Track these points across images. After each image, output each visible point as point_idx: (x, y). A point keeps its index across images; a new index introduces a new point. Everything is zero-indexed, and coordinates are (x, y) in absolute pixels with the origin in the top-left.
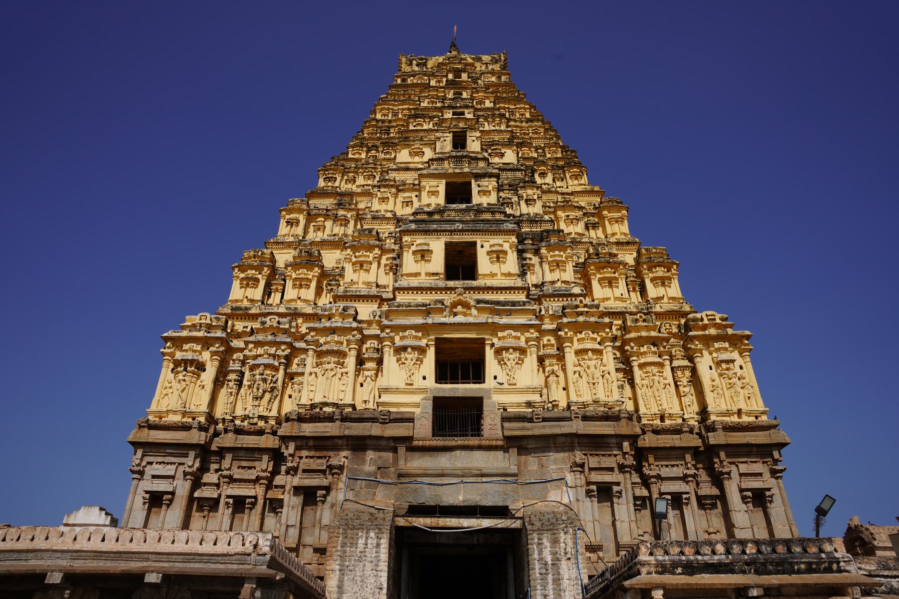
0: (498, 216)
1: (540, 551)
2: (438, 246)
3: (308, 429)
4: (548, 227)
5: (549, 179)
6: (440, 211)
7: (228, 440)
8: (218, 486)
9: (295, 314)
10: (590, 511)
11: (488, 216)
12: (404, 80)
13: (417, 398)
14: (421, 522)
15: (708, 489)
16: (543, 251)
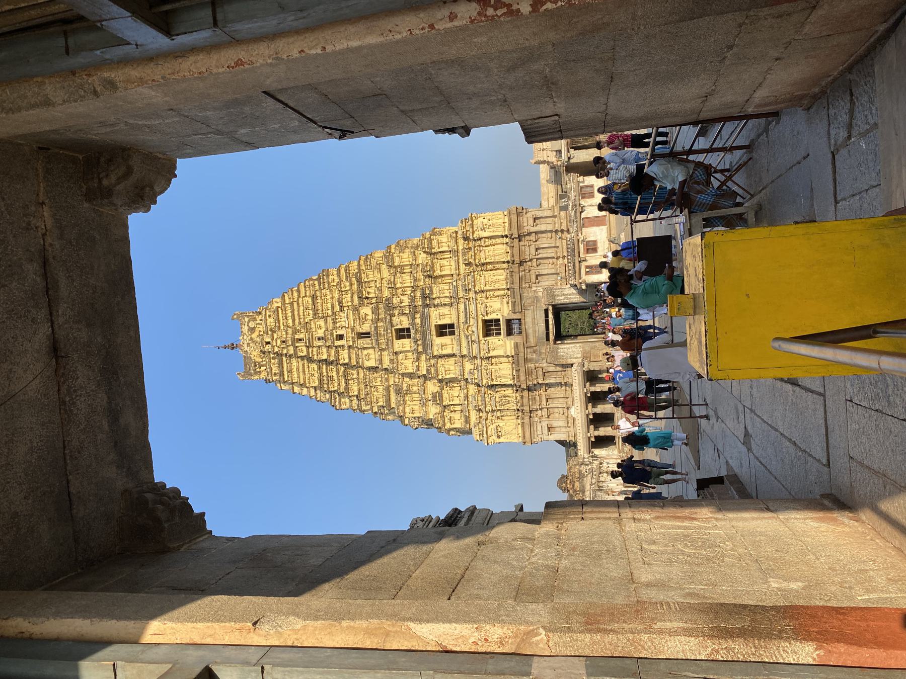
0: (418, 315)
1: (561, 300)
2: (438, 341)
3: (523, 378)
4: (418, 294)
5: (372, 290)
6: (416, 341)
7: (527, 409)
8: (541, 409)
9: (466, 397)
10: (546, 282)
11: (418, 321)
12: (276, 374)
13: (508, 342)
14: (552, 337)
15: (533, 237)
16: (434, 296)
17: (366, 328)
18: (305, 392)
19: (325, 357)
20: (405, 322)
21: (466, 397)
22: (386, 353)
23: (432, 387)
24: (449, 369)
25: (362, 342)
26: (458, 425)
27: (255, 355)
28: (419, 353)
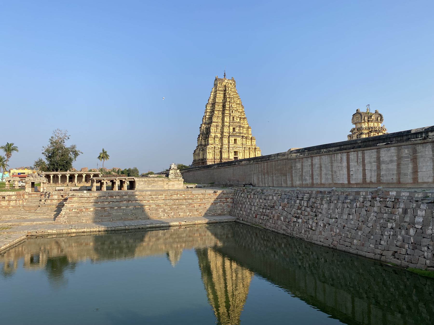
2: (233, 139)
4: (243, 135)
9: (217, 145)
11: (237, 134)
17: (235, 119)
18: (212, 96)
19: (227, 106)
20: (237, 130)
21: (217, 145)
22: (228, 124)
23: (219, 135)
24: (225, 141)
25: (231, 117)
26: (210, 142)
27: (224, 84)
28: (229, 133)
